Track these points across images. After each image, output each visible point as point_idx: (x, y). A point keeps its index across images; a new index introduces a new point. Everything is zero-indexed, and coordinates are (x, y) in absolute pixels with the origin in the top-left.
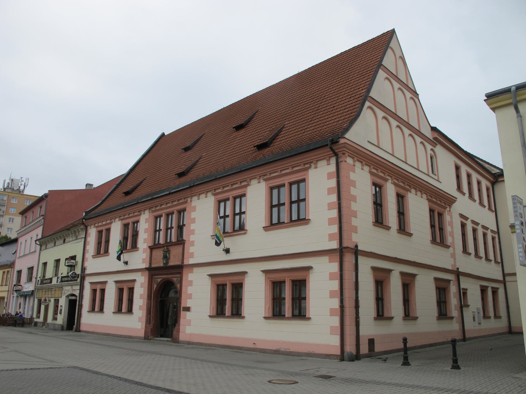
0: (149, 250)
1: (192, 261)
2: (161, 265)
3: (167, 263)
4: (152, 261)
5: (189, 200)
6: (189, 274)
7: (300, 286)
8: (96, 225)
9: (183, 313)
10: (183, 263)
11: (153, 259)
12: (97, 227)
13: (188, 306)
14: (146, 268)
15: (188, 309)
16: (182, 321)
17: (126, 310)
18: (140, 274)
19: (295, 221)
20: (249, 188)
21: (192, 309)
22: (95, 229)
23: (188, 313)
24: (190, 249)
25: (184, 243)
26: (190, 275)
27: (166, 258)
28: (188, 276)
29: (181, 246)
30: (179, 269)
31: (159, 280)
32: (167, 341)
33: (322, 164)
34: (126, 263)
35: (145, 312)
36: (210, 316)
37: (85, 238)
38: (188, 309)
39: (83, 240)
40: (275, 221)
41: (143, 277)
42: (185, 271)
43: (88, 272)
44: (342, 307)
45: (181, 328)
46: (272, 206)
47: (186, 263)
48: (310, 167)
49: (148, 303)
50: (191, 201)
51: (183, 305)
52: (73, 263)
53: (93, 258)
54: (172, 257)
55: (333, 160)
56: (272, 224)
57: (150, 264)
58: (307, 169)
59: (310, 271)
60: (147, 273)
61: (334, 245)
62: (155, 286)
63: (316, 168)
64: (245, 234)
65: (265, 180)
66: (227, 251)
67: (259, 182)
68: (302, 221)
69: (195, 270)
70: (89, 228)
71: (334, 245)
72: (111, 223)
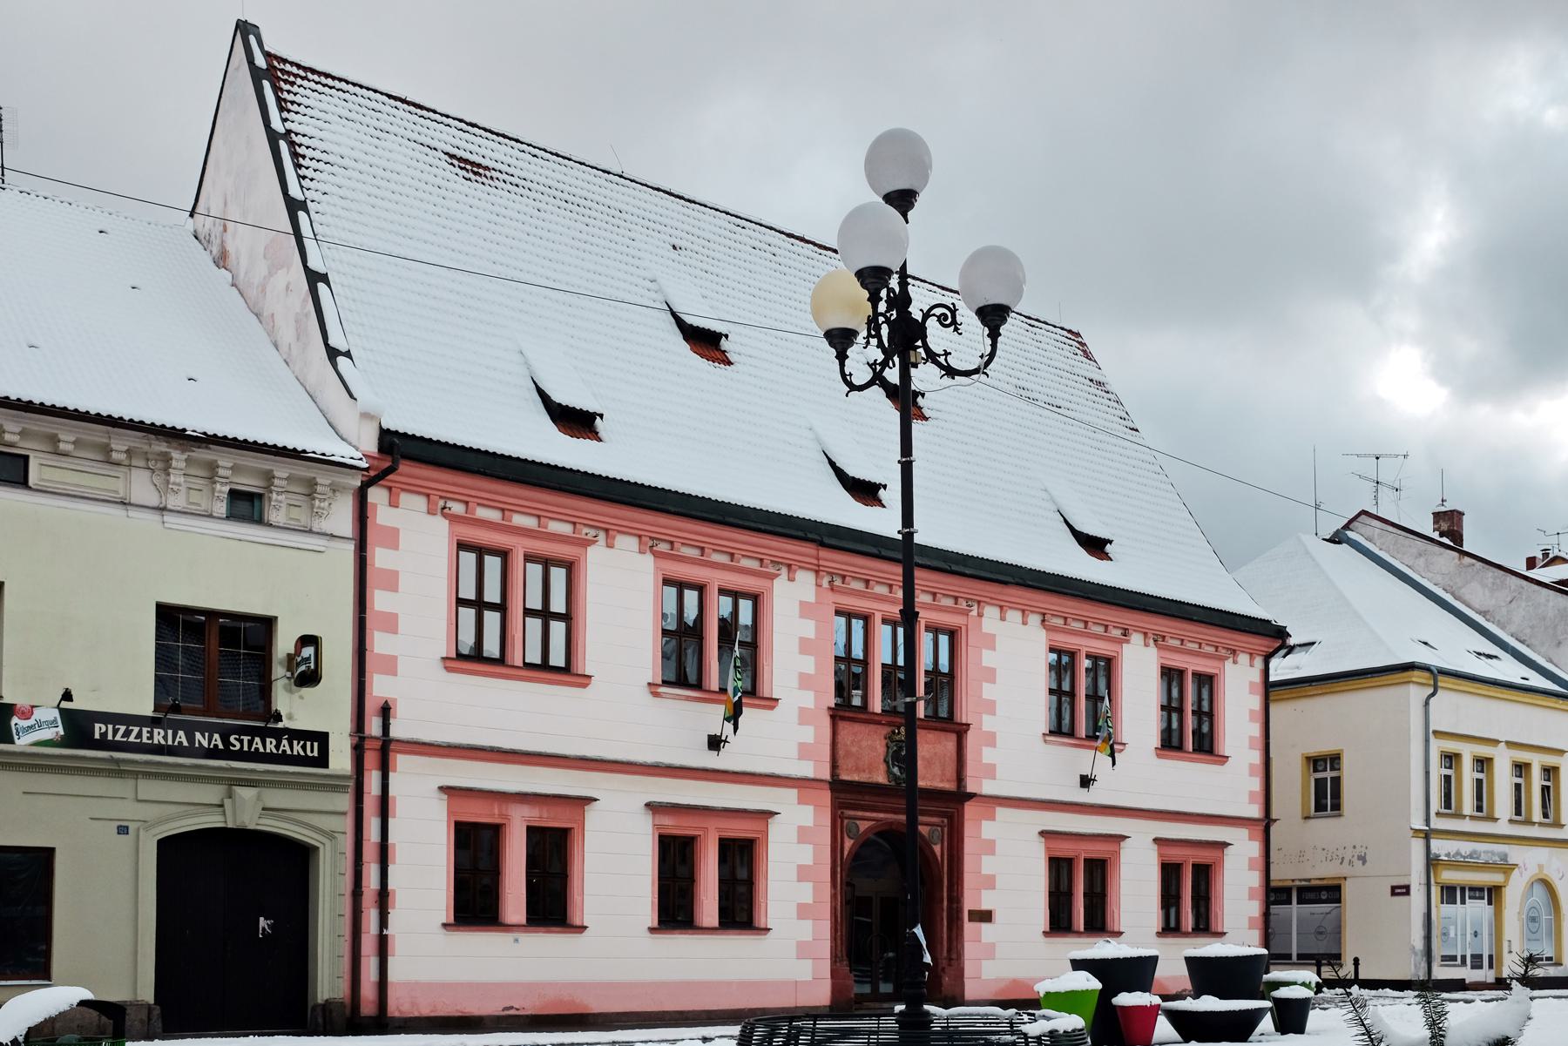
0: (827, 722)
1: (988, 788)
2: (881, 778)
4: (840, 762)
7: (1205, 876)
8: (457, 508)
9: (969, 927)
11: (841, 753)
13: (985, 907)
15: (985, 916)
16: (970, 950)
17: (716, 923)
18: (792, 793)
21: (997, 916)
23: (985, 927)
24: (980, 754)
35: (826, 926)
38: (985, 916)
41: (809, 809)
42: (970, 809)
47: (970, 788)
49: (834, 896)
50: (980, 615)
51: (969, 904)
59: (1226, 851)
60: (826, 796)
62: (848, 843)
67: (1146, 645)
69: (1001, 812)
70: (376, 495)
71: (1255, 811)
72: (586, 543)
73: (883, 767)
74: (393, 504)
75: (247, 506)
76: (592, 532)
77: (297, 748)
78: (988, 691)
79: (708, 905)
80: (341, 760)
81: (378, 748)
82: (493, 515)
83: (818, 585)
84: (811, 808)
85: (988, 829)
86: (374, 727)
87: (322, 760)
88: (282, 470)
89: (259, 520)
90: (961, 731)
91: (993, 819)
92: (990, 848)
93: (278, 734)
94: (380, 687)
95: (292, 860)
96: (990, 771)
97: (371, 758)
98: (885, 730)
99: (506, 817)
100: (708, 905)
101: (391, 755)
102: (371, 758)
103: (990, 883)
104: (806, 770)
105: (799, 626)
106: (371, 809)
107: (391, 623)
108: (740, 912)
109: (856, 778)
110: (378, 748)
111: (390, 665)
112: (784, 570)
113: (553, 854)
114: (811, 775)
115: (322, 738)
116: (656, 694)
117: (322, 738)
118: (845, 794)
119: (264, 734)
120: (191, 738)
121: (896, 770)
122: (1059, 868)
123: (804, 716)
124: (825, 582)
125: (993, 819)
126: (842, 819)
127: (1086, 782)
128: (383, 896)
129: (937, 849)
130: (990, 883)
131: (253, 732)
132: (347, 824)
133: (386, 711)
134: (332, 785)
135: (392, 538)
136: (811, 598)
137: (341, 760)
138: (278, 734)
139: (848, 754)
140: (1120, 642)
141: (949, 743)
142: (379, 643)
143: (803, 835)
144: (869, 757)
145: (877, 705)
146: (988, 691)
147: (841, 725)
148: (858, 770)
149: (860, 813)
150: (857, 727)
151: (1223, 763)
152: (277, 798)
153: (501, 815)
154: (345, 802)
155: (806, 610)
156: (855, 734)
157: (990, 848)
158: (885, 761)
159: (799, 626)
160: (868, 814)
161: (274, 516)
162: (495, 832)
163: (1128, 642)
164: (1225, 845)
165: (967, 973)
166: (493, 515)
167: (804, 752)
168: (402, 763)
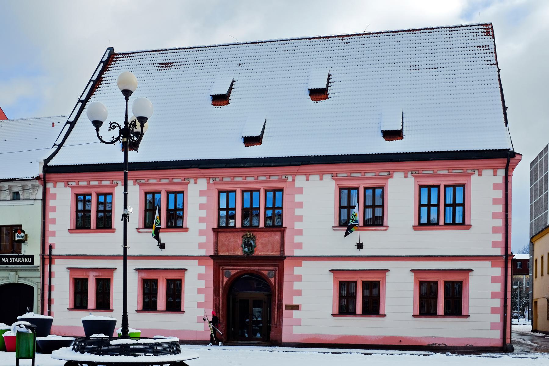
1: (297, 253)
3: (252, 252)
5: (290, 179)
6: (295, 268)
8: (74, 184)
9: (285, 312)
10: (283, 254)
11: (220, 245)
12: (72, 187)
13: (295, 303)
14: (211, 256)
15: (297, 307)
16: (285, 321)
18: (196, 262)
19: (459, 224)
20: (390, 180)
21: (303, 307)
22: (69, 189)
23: (295, 312)
25: (285, 230)
26: (296, 269)
27: (247, 244)
28: (293, 270)
29: (279, 233)
30: (278, 261)
31: (233, 272)
32: (259, 343)
33: (488, 173)
34: (162, 246)
36: (333, 315)
37: (44, 200)
38: (297, 307)
39: (39, 204)
40: (424, 220)
41: (203, 268)
42: (286, 263)
43: (55, 252)
44: (505, 306)
45: (285, 329)
46: (421, 206)
48: (472, 174)
51: (286, 302)
52: (23, 237)
53: (71, 233)
54: (259, 246)
55: (501, 173)
56: (420, 225)
57: (216, 249)
58: (470, 175)
61: (499, 251)
62: (225, 279)
63: (480, 175)
64: (386, 230)
65: (416, 177)
66: (360, 246)
67: (406, 177)
68: (463, 225)
69: (305, 263)
70: (50, 185)
73: (240, 249)
74: (55, 186)
75: (16, 196)
76: (115, 182)
77: (26, 260)
78: (298, 212)
79: (161, 303)
80: (37, 262)
81: (48, 258)
82: (85, 183)
83: (208, 183)
84: (204, 267)
85: (297, 271)
86: (47, 252)
87: (32, 263)
88: (19, 184)
89: (18, 199)
90: (282, 230)
91: (301, 266)
92: (299, 278)
93: (21, 257)
94: (50, 240)
95: (30, 289)
96: (299, 246)
97: (47, 261)
98: (242, 234)
99: (88, 276)
100: (161, 303)
101: (53, 260)
102: (47, 261)
103: (299, 293)
104: (203, 252)
105: (199, 201)
106: (47, 276)
107: (54, 221)
108: (175, 305)
109: (227, 254)
110: (48, 258)
111: (53, 234)
112: (192, 181)
113: (104, 287)
114: (204, 254)
115: (32, 257)
116: (139, 232)
117: (32, 257)
118: (219, 261)
119: (18, 257)
120: (9, 260)
121: (246, 249)
122: (342, 285)
123: (201, 233)
124: (211, 181)
125: (301, 266)
126: (223, 270)
127: (360, 246)
128: (50, 300)
129: (272, 280)
130: (299, 293)
131: (15, 257)
132: (40, 280)
133: (51, 247)
134: (35, 270)
135: (54, 197)
136: (205, 188)
137: (37, 262)
138: (21, 257)
139: (223, 245)
140: (386, 178)
141: (277, 237)
142: (50, 228)
143: (200, 277)
144: (234, 246)
145: (239, 225)
146: (298, 212)
147: (220, 234)
148: (228, 251)
149: (231, 267)
150: (228, 234)
151: (468, 229)
152: (21, 274)
153: (86, 275)
154: (39, 274)
155: (202, 193)
156: (227, 237)
157: (299, 278)
158: (242, 246)
159: (199, 201)
160: (236, 268)
161: (22, 197)
162: (85, 281)
163: (392, 177)
164: (471, 270)
165: (284, 331)
166: (85, 183)
167: (201, 246)
168: (57, 261)
